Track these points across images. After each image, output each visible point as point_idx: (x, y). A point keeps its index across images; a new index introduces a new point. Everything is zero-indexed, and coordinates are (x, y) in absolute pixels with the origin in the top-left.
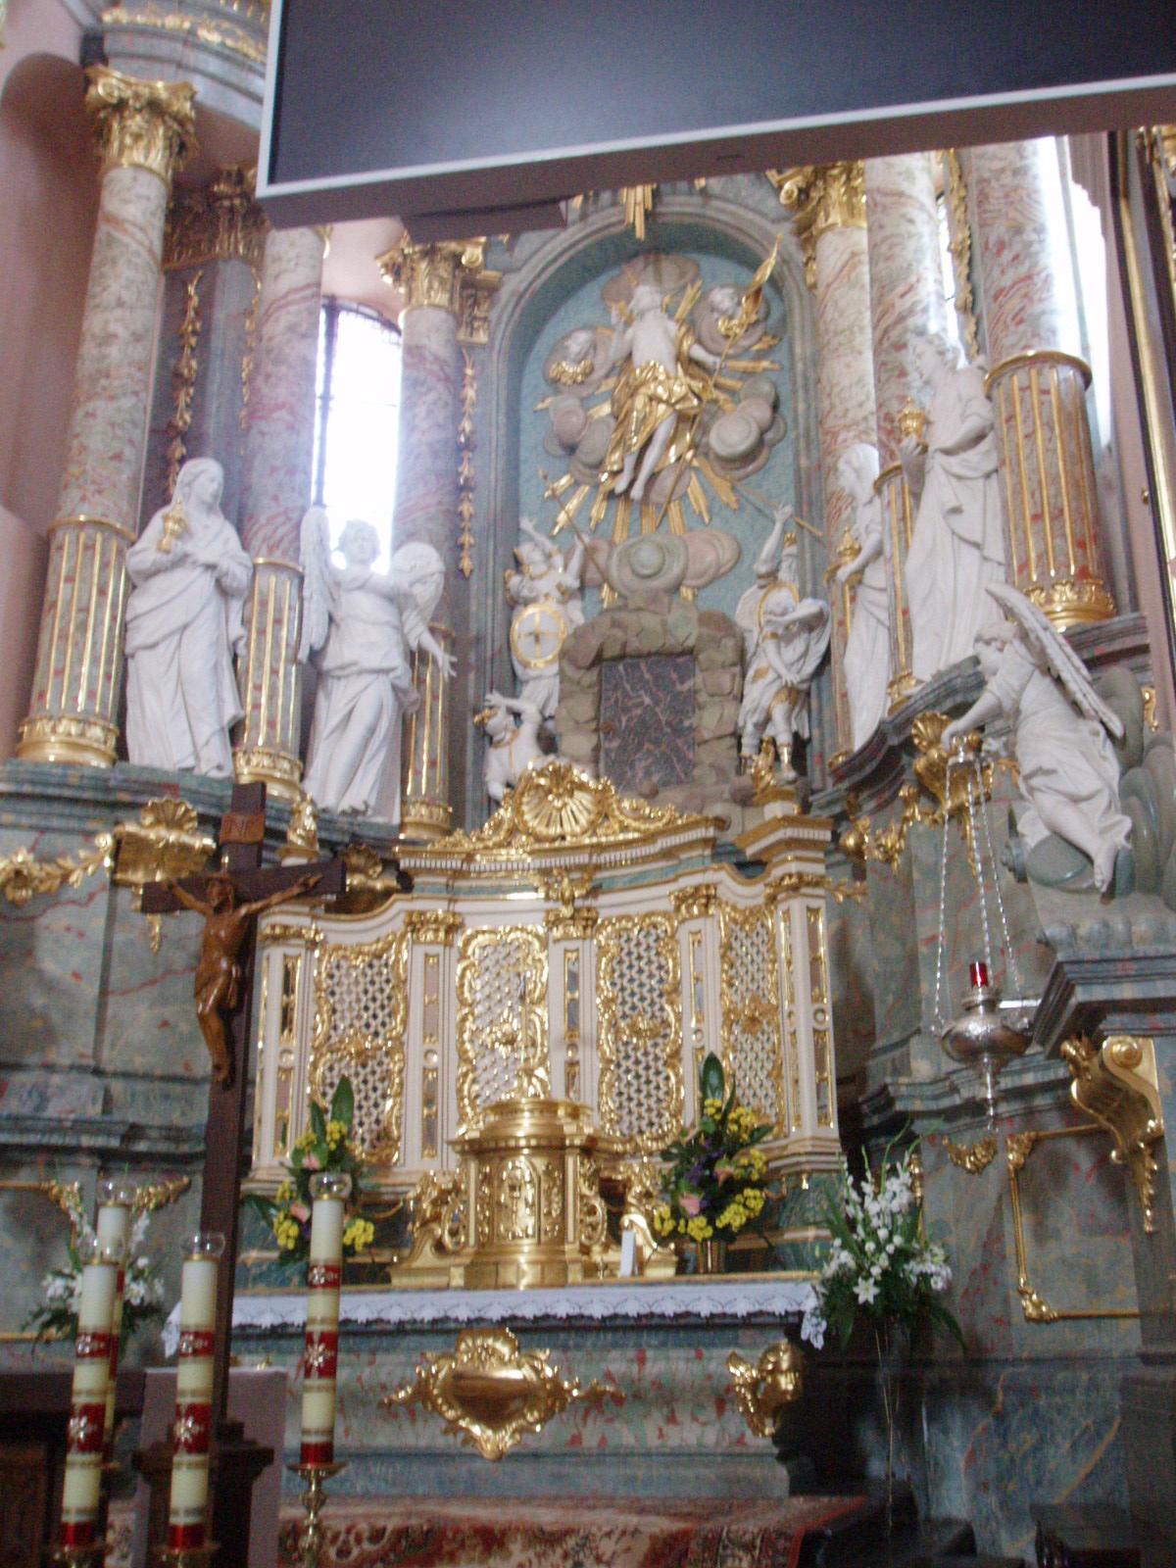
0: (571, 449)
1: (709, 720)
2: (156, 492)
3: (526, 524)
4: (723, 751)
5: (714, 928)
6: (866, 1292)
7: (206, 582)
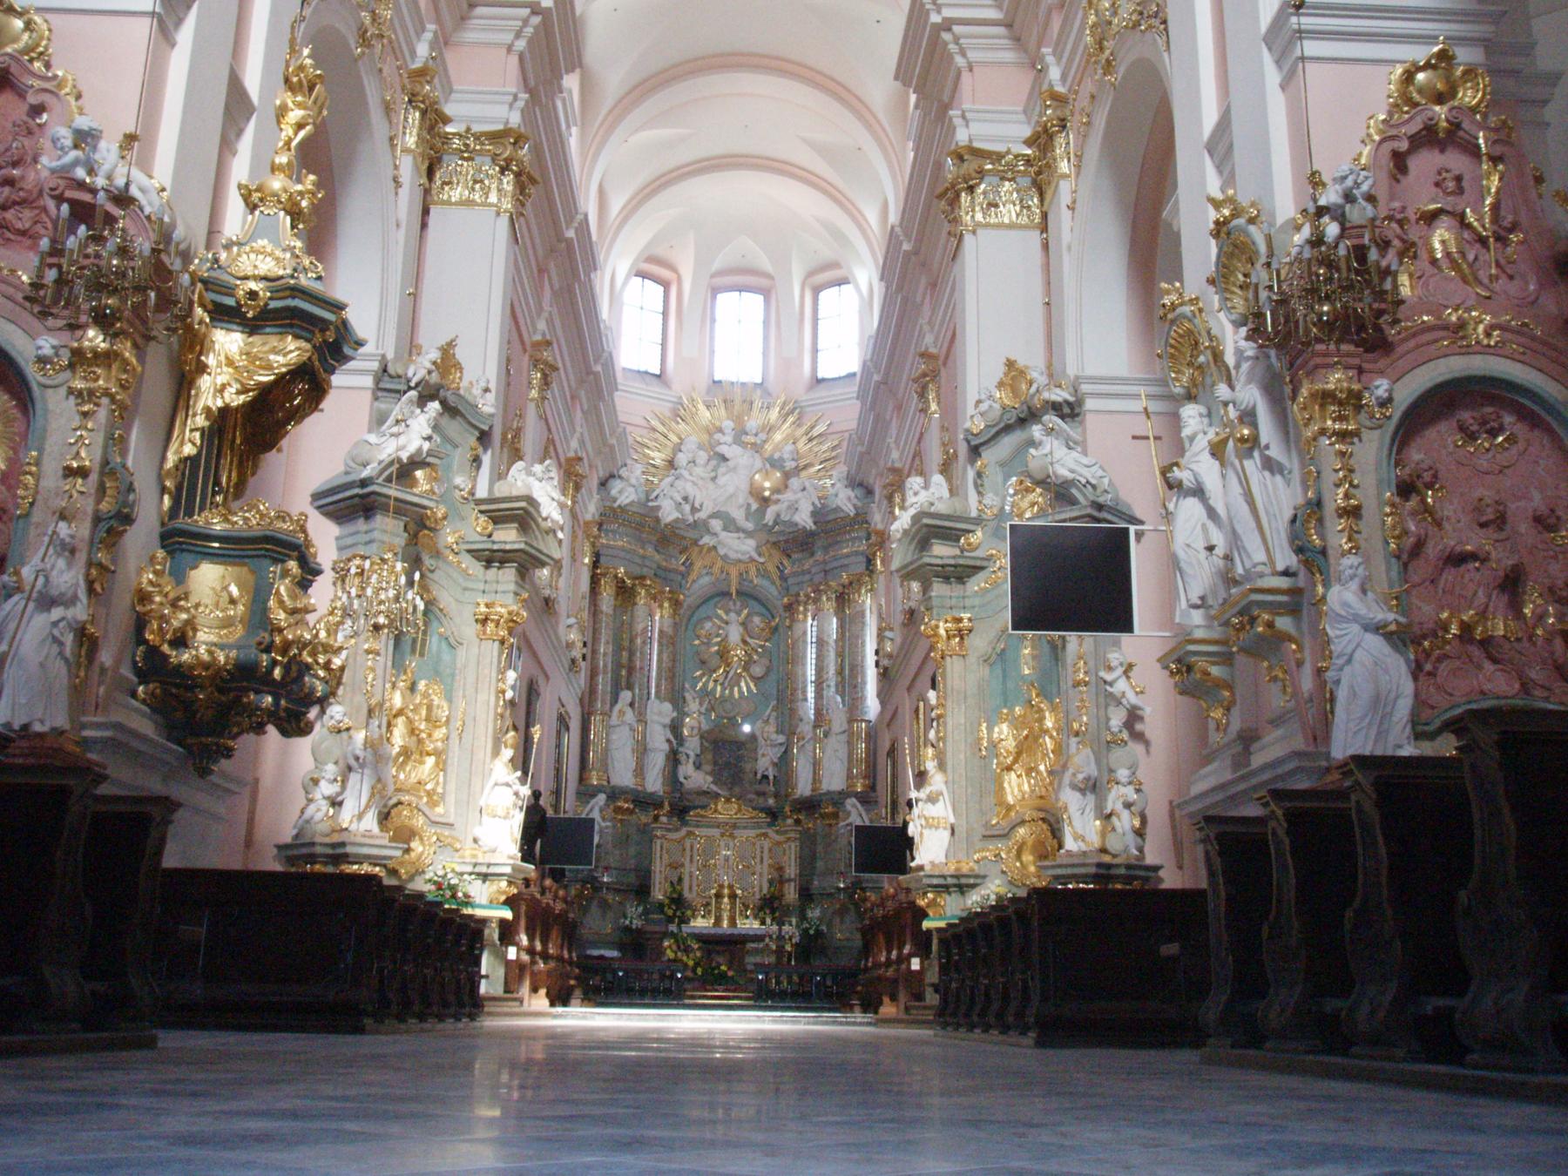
0: (703, 662)
1: (748, 767)
2: (615, 700)
3: (687, 686)
4: (751, 776)
5: (767, 844)
6: (812, 932)
7: (627, 728)
